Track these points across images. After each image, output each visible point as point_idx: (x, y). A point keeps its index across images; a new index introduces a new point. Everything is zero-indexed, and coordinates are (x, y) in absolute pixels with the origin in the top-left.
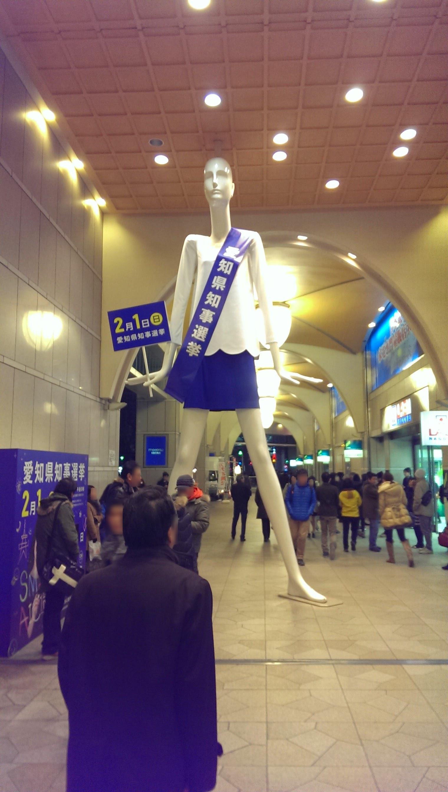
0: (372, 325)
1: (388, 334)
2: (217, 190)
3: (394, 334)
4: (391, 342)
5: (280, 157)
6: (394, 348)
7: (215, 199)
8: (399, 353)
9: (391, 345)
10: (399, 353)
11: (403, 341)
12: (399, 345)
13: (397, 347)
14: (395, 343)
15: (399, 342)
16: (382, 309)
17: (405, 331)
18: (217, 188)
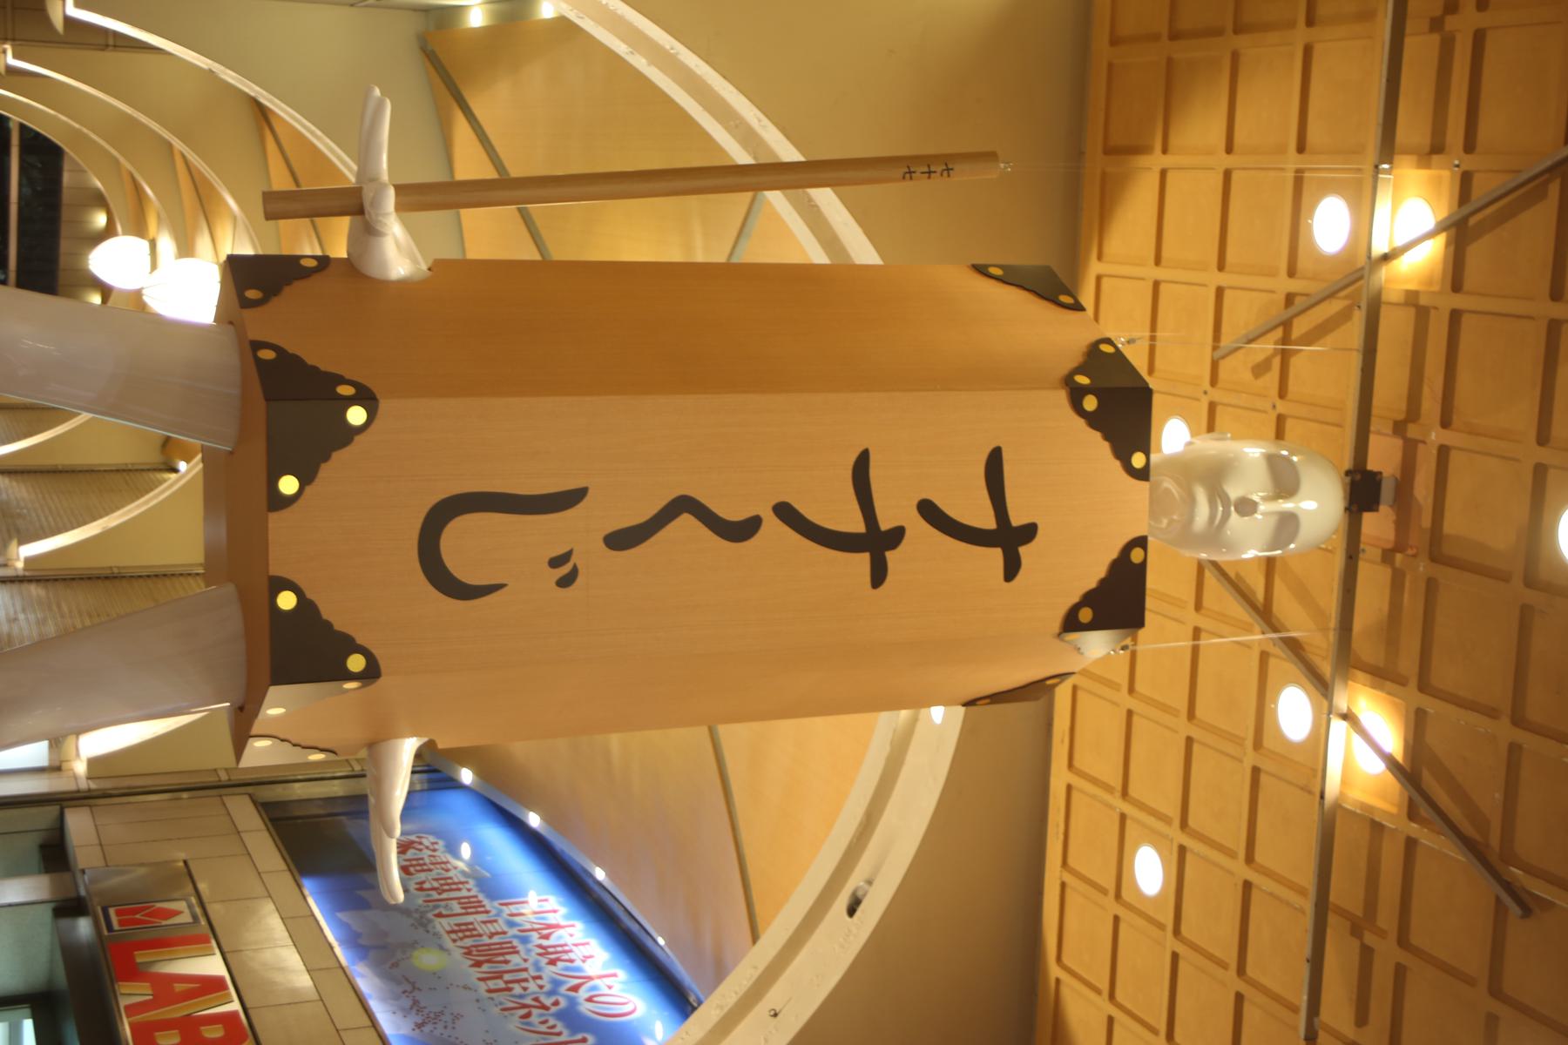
0: (534, 820)
1: (494, 888)
2: (1226, 515)
3: (501, 925)
4: (472, 906)
5: (1294, 711)
6: (444, 924)
7: (1191, 501)
8: (427, 959)
9: (457, 908)
10: (427, 959)
11: (475, 973)
12: (458, 954)
13: (449, 944)
14: (465, 930)
15: (468, 952)
16: (600, 874)
17: (517, 989)
18: (1234, 516)
